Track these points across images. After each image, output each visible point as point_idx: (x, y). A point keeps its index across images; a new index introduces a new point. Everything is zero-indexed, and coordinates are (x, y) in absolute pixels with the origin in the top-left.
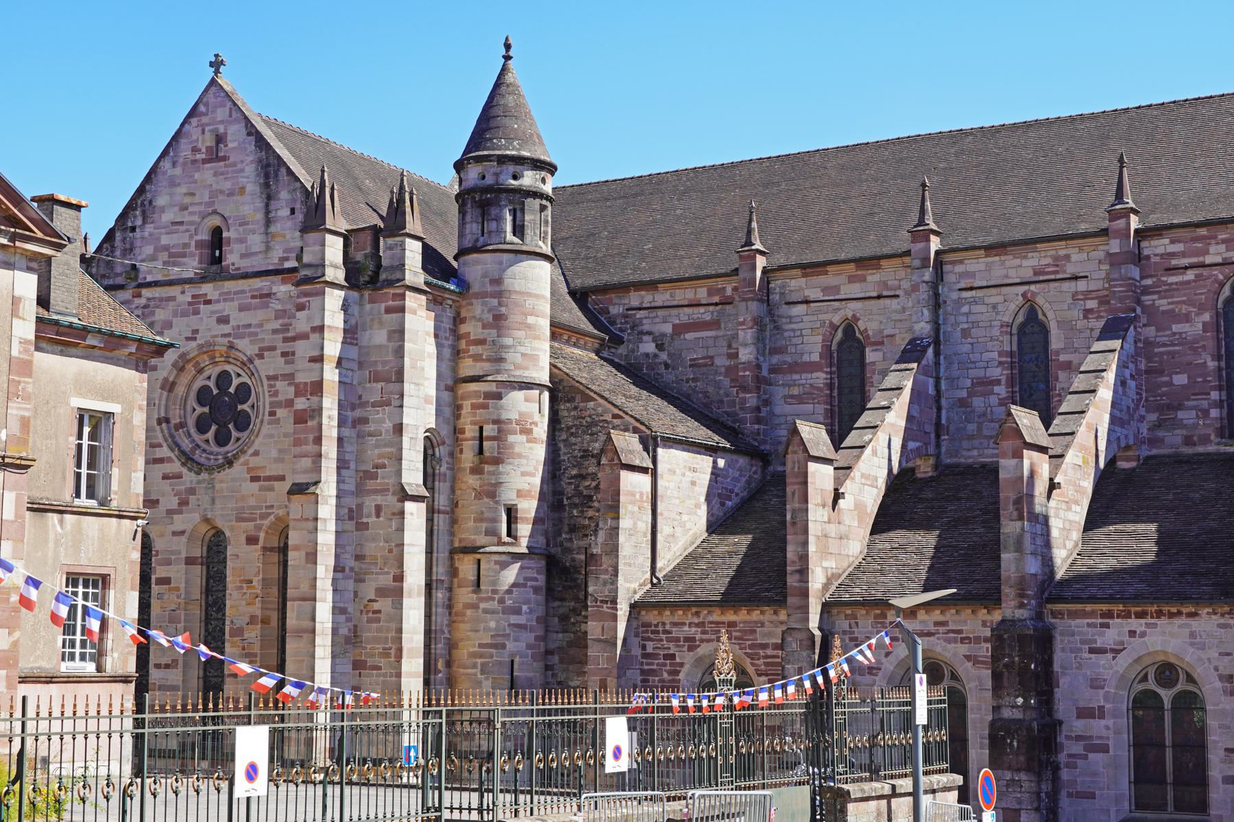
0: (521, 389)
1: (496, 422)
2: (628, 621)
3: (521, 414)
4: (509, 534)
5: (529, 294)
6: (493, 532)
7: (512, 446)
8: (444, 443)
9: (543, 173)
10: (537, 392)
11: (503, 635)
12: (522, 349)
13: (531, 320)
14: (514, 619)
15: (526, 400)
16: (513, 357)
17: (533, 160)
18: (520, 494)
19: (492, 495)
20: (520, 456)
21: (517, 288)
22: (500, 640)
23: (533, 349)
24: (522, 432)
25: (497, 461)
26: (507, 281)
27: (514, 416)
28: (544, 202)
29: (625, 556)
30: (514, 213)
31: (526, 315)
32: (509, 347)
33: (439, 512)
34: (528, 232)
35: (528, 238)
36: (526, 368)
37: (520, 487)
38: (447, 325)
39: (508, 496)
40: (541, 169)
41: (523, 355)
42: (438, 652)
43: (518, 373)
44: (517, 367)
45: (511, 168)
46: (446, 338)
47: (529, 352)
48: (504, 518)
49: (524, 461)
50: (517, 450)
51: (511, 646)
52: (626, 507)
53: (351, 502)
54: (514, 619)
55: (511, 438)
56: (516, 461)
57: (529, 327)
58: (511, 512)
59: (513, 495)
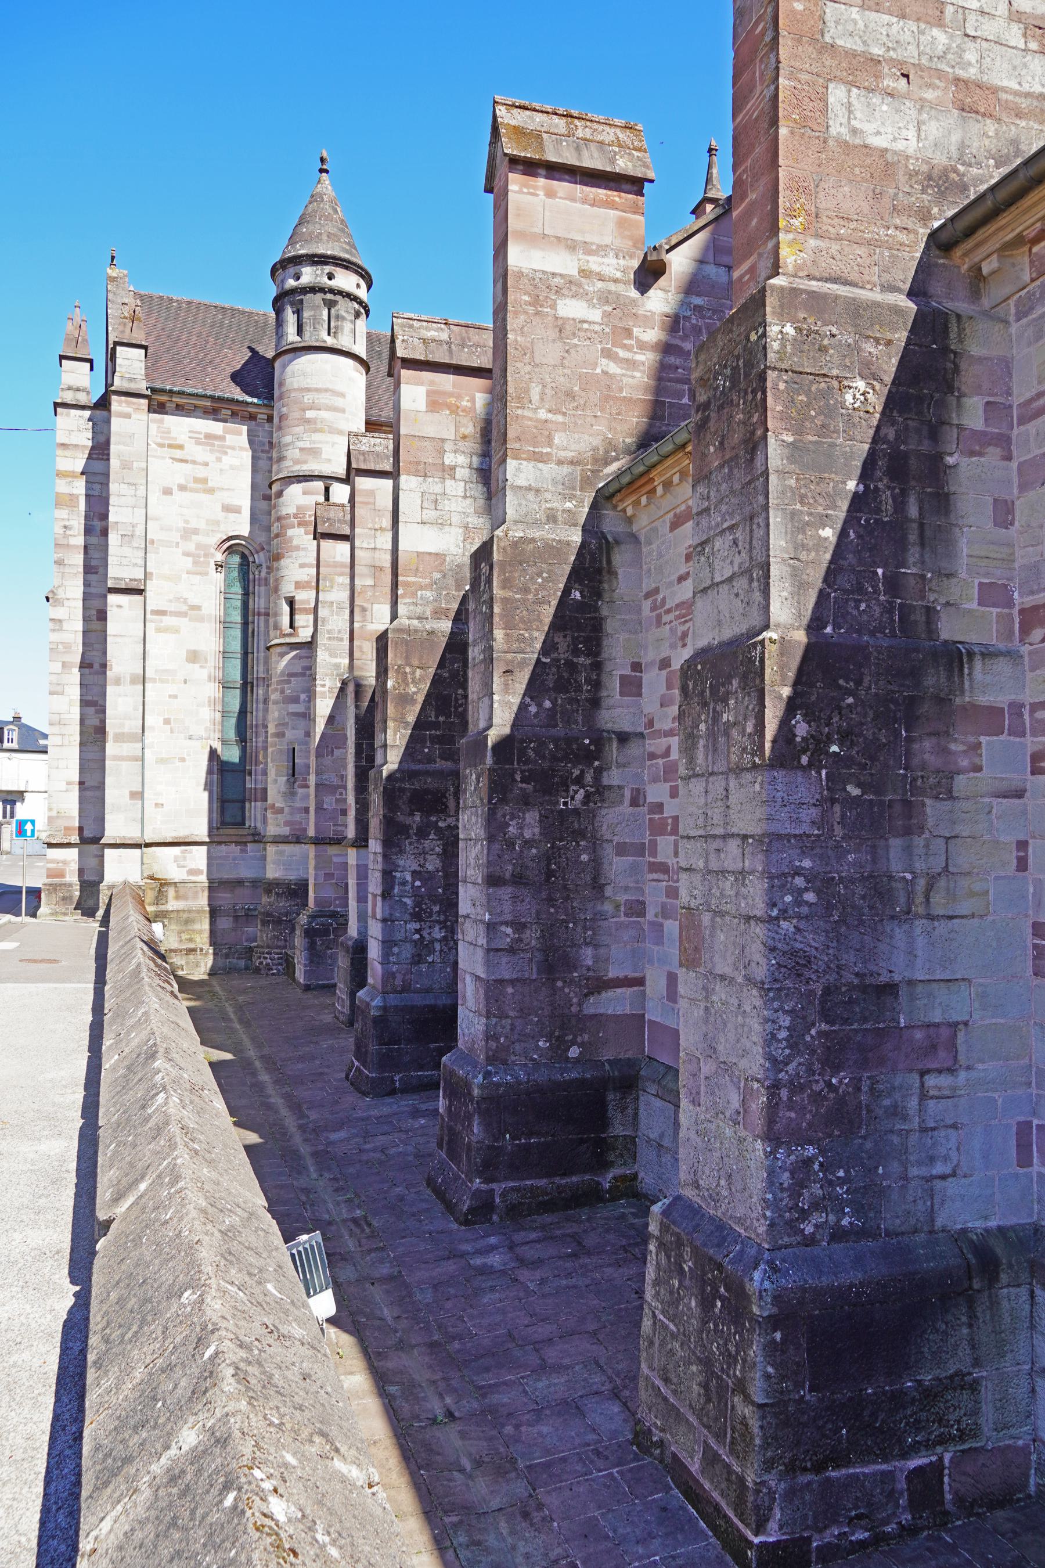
0: (299, 482)
1: (279, 519)
2: (338, 697)
3: (298, 508)
4: (292, 626)
5: (308, 390)
6: (276, 627)
7: (291, 539)
8: (263, 549)
9: (328, 269)
10: (320, 485)
11: (283, 724)
12: (301, 444)
13: (310, 414)
14: (293, 708)
15: (304, 493)
16: (292, 453)
17: (307, 255)
18: (298, 585)
19: (276, 589)
20: (298, 548)
21: (296, 386)
22: (281, 729)
23: (314, 442)
24: (300, 525)
25: (278, 557)
26: (288, 381)
27: (291, 510)
28: (329, 296)
29: (329, 632)
30: (298, 312)
31: (304, 410)
32: (288, 445)
33: (259, 614)
34: (307, 329)
35: (307, 335)
36: (305, 462)
37: (298, 579)
38: (263, 437)
39: (287, 588)
40: (326, 263)
41: (301, 449)
42: (260, 744)
43: (296, 468)
44: (296, 462)
45: (292, 270)
46: (263, 451)
47: (308, 445)
48: (286, 609)
49: (302, 553)
50: (295, 543)
51: (290, 734)
52: (332, 581)
53: (96, 603)
54: (293, 708)
55: (290, 532)
56: (294, 554)
57: (308, 421)
58: (291, 602)
59: (291, 587)
